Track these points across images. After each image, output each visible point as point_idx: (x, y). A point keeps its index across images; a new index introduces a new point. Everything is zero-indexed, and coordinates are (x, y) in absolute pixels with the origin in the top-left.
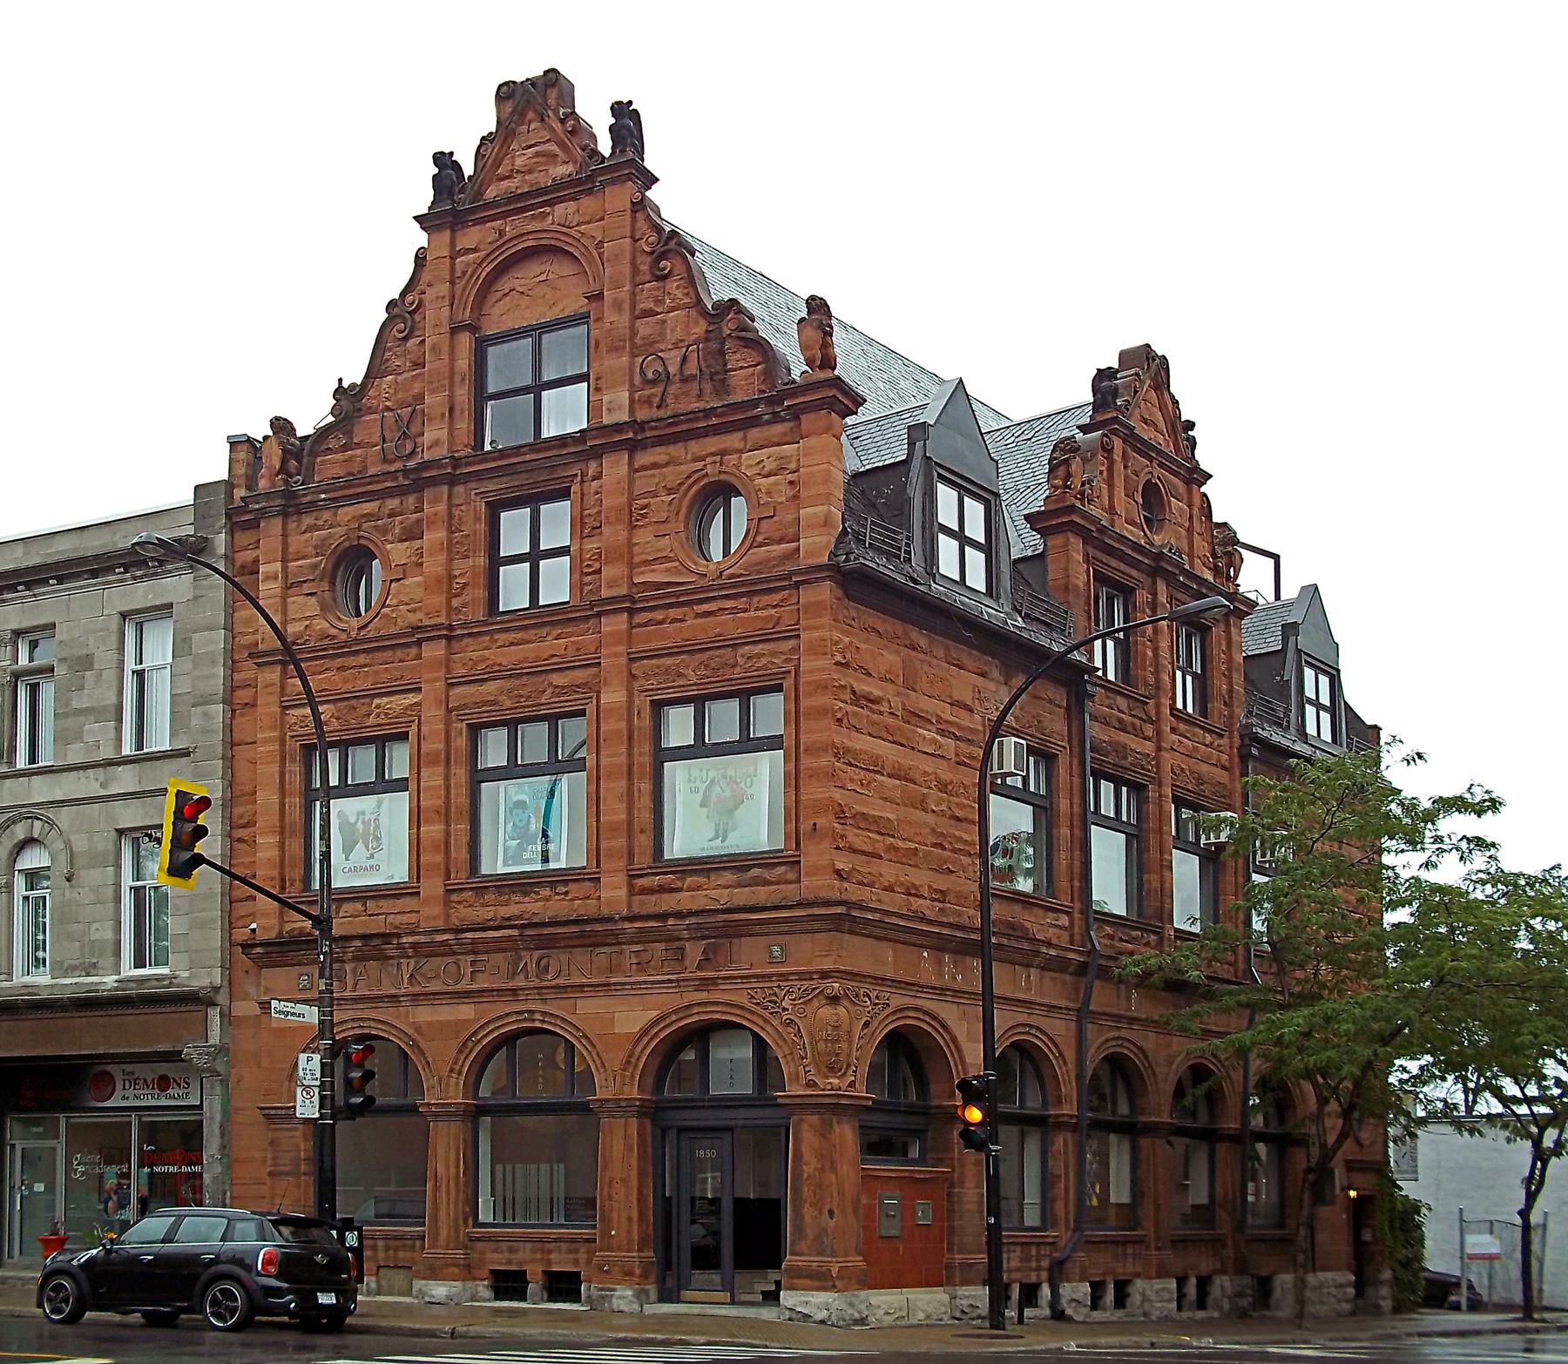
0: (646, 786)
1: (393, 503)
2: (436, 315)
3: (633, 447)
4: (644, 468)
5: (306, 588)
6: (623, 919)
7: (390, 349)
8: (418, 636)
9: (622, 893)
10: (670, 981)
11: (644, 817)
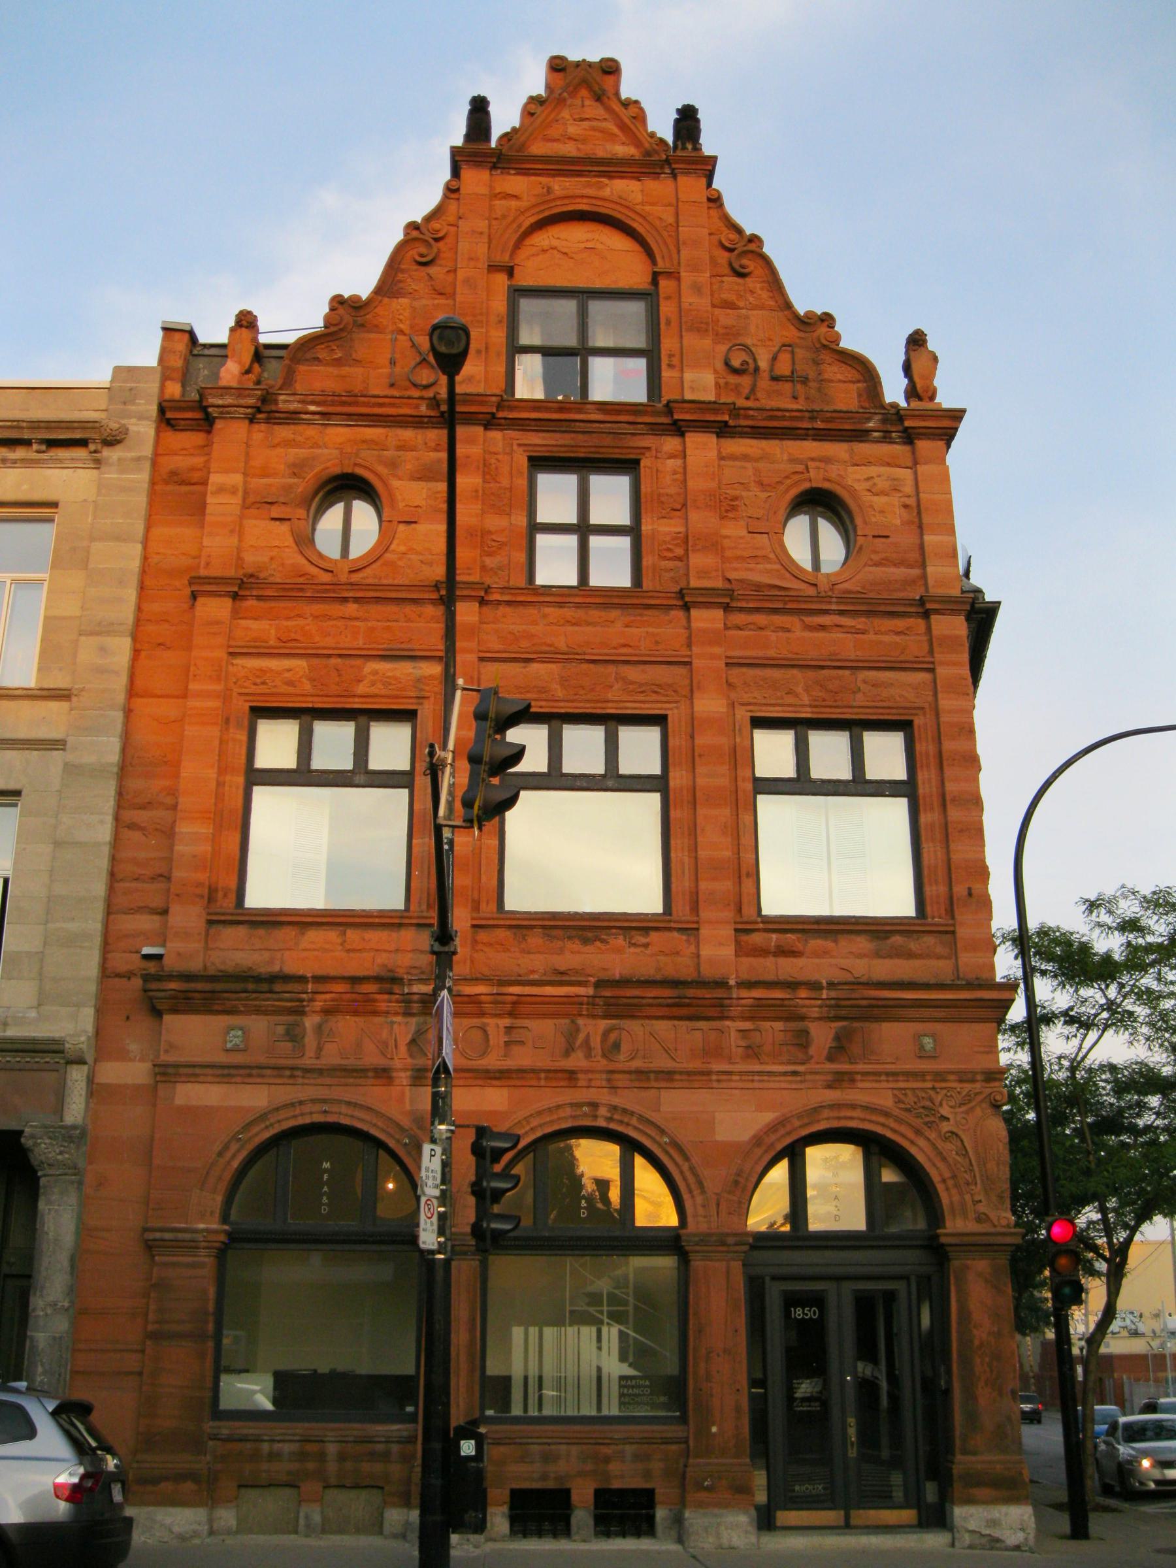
5: (276, 512)
7: (402, 271)
10: (795, 1073)
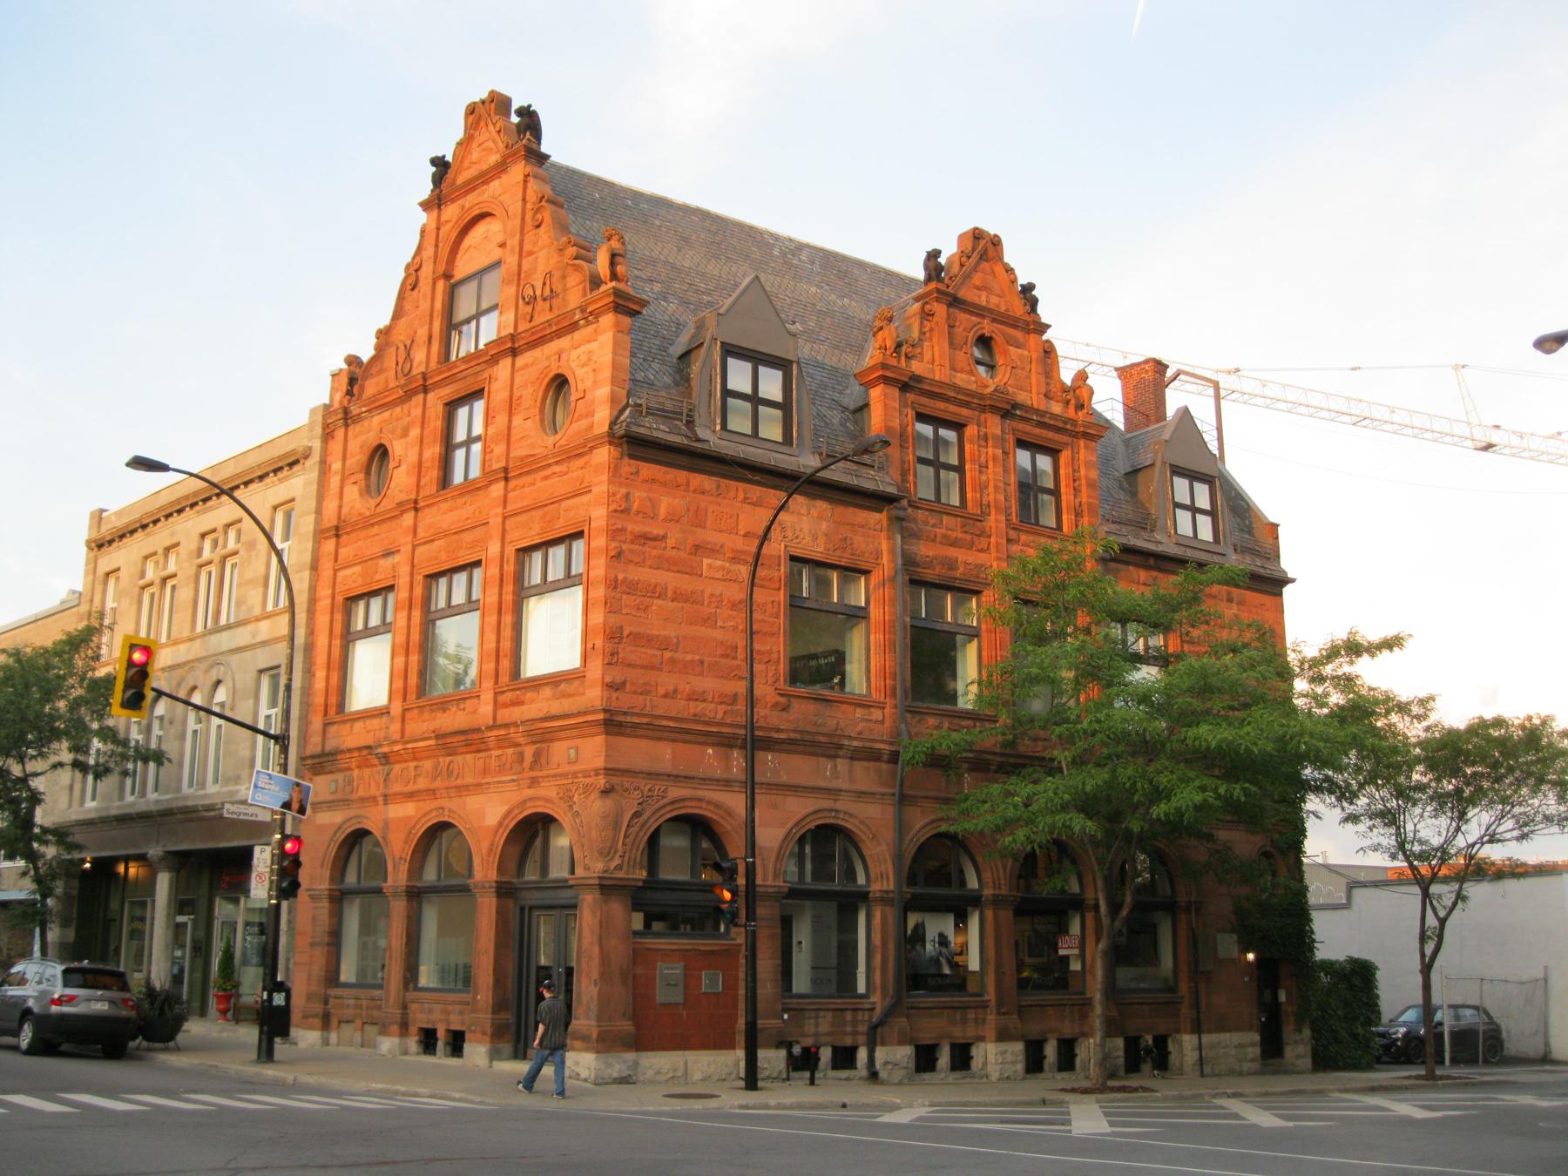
0: (508, 619)
1: (398, 409)
2: (427, 271)
3: (514, 352)
4: (521, 369)
6: (490, 728)
8: (401, 508)
9: (490, 708)
11: (506, 644)
